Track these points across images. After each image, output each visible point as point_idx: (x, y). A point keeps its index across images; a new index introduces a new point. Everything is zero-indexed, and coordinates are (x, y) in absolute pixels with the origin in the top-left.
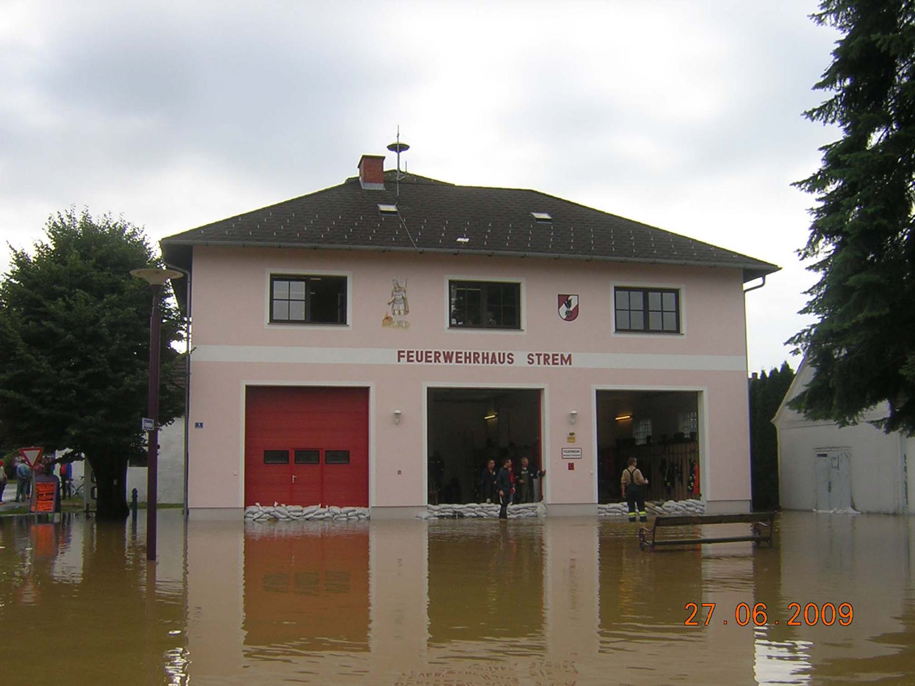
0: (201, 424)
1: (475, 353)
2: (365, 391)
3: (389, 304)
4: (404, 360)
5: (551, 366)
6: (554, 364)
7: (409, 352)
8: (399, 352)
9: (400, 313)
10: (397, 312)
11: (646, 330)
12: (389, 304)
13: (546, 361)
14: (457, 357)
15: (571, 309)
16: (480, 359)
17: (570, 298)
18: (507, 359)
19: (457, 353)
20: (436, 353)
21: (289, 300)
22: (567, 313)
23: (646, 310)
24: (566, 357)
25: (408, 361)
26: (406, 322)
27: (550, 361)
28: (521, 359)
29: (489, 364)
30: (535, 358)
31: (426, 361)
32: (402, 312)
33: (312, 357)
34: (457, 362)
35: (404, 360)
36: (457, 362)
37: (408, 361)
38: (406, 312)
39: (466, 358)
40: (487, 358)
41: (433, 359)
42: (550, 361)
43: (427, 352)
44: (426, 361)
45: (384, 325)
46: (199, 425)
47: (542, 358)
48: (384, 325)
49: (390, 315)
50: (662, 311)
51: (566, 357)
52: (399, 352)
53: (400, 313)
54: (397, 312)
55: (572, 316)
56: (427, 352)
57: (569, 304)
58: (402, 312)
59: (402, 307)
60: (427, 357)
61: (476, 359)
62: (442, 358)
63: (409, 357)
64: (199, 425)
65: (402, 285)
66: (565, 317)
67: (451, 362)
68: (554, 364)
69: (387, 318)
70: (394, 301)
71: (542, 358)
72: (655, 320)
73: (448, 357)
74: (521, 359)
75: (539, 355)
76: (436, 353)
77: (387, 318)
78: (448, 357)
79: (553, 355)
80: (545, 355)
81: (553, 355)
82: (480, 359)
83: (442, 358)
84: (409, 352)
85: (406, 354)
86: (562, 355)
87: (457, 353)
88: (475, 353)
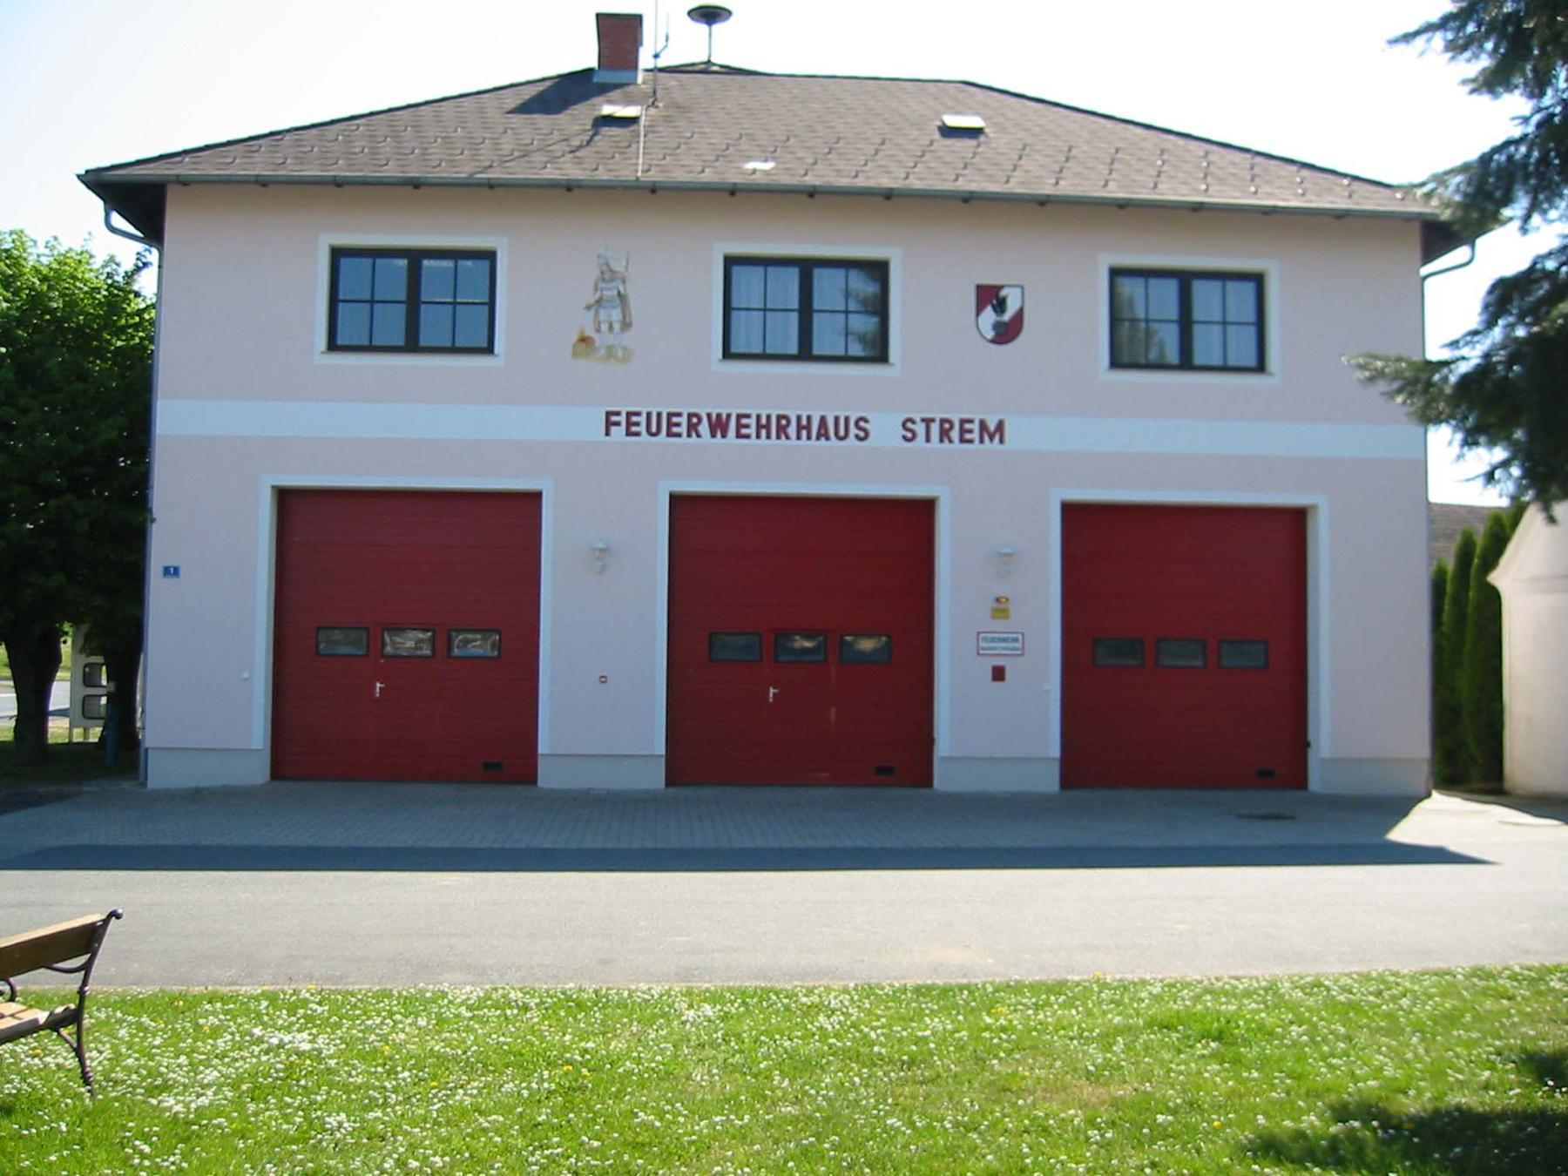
0: (176, 570)
1: (779, 417)
2: (535, 498)
3: (588, 308)
4: (618, 432)
5: (794, 441)
6: (962, 440)
7: (629, 414)
8: (609, 414)
9: (611, 328)
10: (604, 327)
11: (412, 345)
12: (588, 308)
13: (945, 434)
14: (739, 426)
15: (1007, 317)
16: (792, 430)
17: (1003, 293)
18: (853, 431)
19: (739, 417)
20: (690, 416)
21: (454, 304)
22: (997, 326)
23: (413, 302)
24: (992, 427)
25: (629, 433)
26: (624, 349)
27: (955, 434)
28: (885, 430)
29: (813, 442)
30: (920, 429)
31: (670, 434)
32: (617, 326)
33: (409, 427)
34: (739, 436)
35: (618, 432)
36: (739, 436)
37: (629, 433)
38: (626, 325)
39: (759, 427)
40: (808, 428)
41: (683, 429)
42: (955, 434)
43: (670, 415)
44: (670, 434)
45: (576, 354)
46: (171, 572)
47: (935, 428)
48: (576, 354)
49: (590, 332)
50: (372, 302)
51: (992, 427)
52: (609, 414)
53: (611, 328)
54: (604, 327)
55: (1007, 332)
56: (670, 415)
57: (1000, 307)
58: (617, 326)
59: (616, 315)
60: (670, 425)
61: (782, 430)
62: (704, 428)
63: (629, 424)
64: (171, 572)
65: (618, 267)
66: (990, 334)
67: (724, 436)
68: (962, 440)
69: (583, 340)
70: (599, 302)
71: (935, 428)
72: (433, 326)
73: (719, 426)
74: (885, 430)
75: (928, 422)
76: (690, 416)
77: (583, 340)
78: (719, 426)
79: (963, 422)
80: (943, 421)
81: (963, 422)
82: (792, 430)
83: (704, 428)
84: (629, 414)
85: (622, 419)
86: (758, 417)
87: (739, 417)
88: (779, 417)
